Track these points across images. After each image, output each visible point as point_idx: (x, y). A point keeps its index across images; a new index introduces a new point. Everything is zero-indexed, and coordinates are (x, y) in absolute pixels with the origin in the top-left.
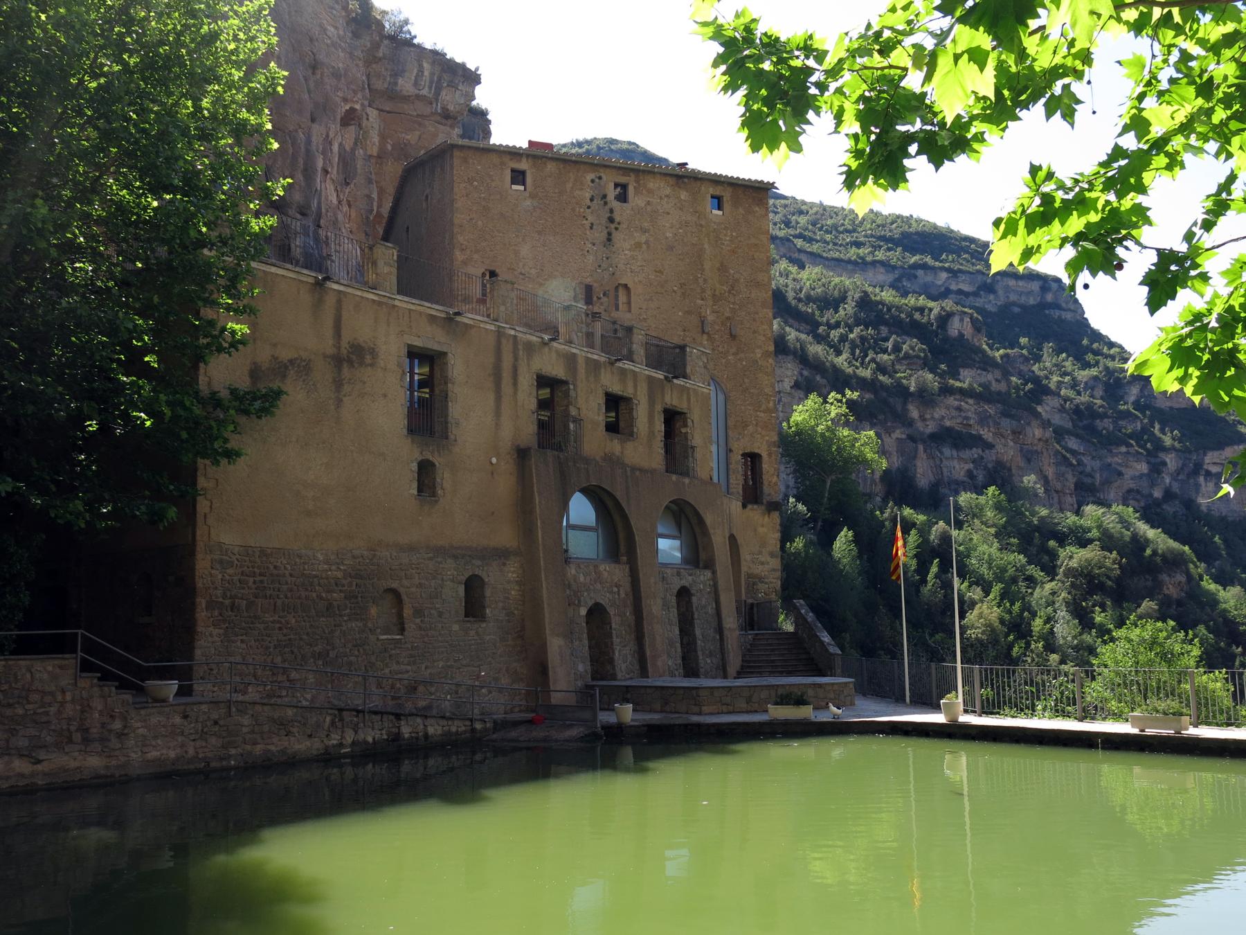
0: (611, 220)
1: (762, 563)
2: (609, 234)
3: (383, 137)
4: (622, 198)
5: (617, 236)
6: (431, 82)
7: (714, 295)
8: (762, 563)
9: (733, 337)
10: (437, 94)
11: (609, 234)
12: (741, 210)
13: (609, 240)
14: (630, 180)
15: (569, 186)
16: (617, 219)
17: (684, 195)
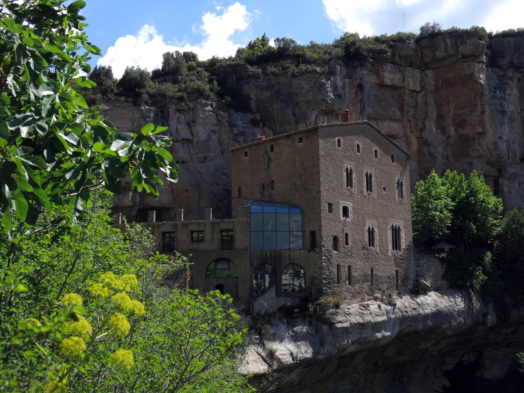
0: (269, 159)
1: (316, 272)
3: (436, 80)
4: (272, 150)
5: (271, 164)
6: (452, 46)
8: (316, 272)
9: (306, 189)
10: (457, 50)
12: (309, 140)
14: (274, 143)
16: (271, 158)
17: (290, 142)
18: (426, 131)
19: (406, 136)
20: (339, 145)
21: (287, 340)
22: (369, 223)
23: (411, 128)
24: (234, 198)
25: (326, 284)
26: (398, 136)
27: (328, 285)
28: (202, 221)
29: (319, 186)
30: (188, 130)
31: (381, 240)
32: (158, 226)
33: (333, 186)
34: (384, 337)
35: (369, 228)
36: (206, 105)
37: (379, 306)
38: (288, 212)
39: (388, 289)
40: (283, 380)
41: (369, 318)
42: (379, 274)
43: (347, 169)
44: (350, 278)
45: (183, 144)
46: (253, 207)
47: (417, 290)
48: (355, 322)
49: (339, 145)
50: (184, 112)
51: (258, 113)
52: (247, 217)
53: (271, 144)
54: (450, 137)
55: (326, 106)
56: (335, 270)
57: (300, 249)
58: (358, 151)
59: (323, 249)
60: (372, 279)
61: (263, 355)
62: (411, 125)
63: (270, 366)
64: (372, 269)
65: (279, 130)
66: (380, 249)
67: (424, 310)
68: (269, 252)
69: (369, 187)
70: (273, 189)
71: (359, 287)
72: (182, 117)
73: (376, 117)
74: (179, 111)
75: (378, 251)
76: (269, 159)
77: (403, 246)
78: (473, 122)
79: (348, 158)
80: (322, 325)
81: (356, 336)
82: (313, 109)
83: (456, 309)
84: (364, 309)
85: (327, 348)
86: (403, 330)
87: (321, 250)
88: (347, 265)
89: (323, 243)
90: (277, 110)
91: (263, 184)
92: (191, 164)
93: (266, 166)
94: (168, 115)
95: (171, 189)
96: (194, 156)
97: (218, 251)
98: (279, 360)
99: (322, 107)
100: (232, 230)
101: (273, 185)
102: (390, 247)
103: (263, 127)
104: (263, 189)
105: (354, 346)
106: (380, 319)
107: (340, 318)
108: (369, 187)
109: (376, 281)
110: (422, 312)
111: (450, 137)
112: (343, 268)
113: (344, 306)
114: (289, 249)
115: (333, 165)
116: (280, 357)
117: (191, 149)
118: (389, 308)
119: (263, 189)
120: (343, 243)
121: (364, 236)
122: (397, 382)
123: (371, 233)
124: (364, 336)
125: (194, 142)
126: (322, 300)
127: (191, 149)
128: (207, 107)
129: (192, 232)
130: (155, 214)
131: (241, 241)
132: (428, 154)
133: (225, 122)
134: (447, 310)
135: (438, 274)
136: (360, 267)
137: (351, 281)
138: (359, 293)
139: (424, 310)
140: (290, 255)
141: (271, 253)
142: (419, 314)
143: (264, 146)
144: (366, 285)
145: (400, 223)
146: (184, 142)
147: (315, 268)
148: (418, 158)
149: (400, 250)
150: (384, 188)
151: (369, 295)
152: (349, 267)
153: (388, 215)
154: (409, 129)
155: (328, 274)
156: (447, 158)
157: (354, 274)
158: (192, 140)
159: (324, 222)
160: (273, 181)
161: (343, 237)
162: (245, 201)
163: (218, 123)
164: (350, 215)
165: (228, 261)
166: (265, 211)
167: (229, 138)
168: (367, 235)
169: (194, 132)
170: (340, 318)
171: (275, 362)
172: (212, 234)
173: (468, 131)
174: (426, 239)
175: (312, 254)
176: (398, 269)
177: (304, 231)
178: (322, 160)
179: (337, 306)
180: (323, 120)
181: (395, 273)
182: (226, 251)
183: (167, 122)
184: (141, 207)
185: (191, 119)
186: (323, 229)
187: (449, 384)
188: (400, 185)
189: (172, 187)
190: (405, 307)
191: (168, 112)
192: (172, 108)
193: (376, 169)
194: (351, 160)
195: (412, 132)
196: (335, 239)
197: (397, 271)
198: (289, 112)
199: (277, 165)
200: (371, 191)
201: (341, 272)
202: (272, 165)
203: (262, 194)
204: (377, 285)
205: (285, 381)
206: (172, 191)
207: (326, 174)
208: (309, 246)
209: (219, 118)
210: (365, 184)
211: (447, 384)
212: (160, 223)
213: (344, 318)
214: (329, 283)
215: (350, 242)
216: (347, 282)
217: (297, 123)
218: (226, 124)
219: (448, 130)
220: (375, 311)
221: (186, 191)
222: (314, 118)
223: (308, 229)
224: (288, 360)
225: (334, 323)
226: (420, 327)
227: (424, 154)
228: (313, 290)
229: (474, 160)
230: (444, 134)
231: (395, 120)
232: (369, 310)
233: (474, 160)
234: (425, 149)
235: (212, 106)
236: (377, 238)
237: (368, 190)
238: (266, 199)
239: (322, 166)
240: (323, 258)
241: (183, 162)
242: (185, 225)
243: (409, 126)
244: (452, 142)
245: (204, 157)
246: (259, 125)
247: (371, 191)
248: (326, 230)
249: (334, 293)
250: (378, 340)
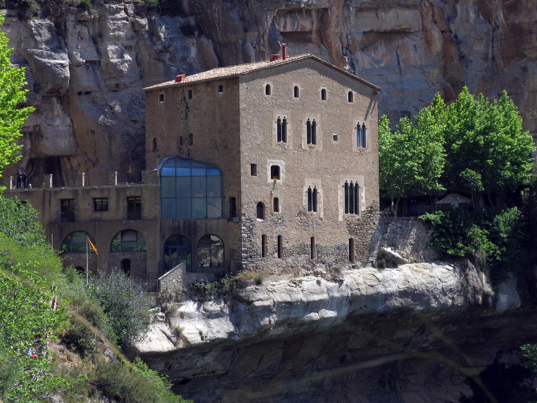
0: (187, 107)
1: (236, 244)
2: (187, 114)
4: (190, 97)
5: (188, 115)
7: (219, 130)
8: (236, 244)
9: (226, 148)
11: (187, 114)
12: (229, 89)
13: (187, 116)
15: (175, 97)
16: (189, 106)
17: (209, 89)
18: (458, 20)
19: (424, 29)
20: (268, 92)
21: (197, 319)
22: (309, 183)
23: (433, 16)
24: (149, 152)
25: (246, 258)
26: (411, 31)
27: (249, 259)
28: (105, 187)
29: (239, 145)
30: (94, 48)
31: (327, 202)
32: (56, 193)
33: (258, 143)
34: (323, 320)
35: (309, 190)
36: (118, 11)
37: (319, 283)
38: (204, 174)
39: (336, 262)
40: (196, 364)
41: (299, 296)
42: (323, 244)
43: (279, 120)
44: (280, 250)
45: (87, 67)
46: (165, 169)
47: (387, 262)
48: (280, 300)
49: (268, 92)
50: (86, 24)
51: (193, 15)
52: (157, 183)
53: (190, 89)
54: (498, 27)
55: (286, 5)
56: (259, 242)
57: (219, 218)
58: (296, 95)
59: (243, 218)
60: (312, 249)
61: (169, 333)
62: (433, 12)
63: (175, 344)
64: (312, 239)
65: (221, 40)
66: (324, 214)
67: (385, 287)
68: (182, 222)
69: (311, 138)
70: (191, 144)
71: (293, 260)
72: (85, 30)
73: (375, 6)
74: (80, 22)
75: (322, 216)
76: (187, 107)
78: (530, 5)
79: (280, 107)
80: (239, 303)
81: (282, 316)
82: (268, 10)
83: (439, 287)
84: (294, 285)
85: (244, 328)
86: (354, 311)
87: (240, 219)
88: (277, 235)
89: (243, 211)
90: (218, 12)
91: (181, 138)
92: (98, 95)
93: (184, 115)
94: (66, 30)
95: (71, 130)
96: (102, 83)
97: (124, 222)
98: (185, 340)
99: (281, 6)
100: (140, 197)
101: (192, 139)
102: (341, 210)
103: (199, 36)
104: (181, 144)
105: (282, 328)
106: (316, 298)
107: (260, 296)
108: (311, 138)
109: (318, 252)
110: (382, 290)
111: (498, 27)
112: (270, 238)
113: (268, 283)
114: (206, 218)
115: (258, 117)
116: (186, 335)
117: (98, 73)
118: (332, 284)
119: (181, 144)
120: (271, 209)
121: (302, 199)
122: (387, 387)
123: (312, 195)
124: (293, 316)
125: (102, 64)
126: (240, 276)
127: (98, 73)
128: (119, 13)
129: (95, 199)
130: (51, 179)
131: (150, 209)
132: (457, 57)
133: (144, 33)
134: (424, 288)
135: (420, 242)
136: (294, 236)
137: (281, 254)
138: (292, 267)
139: (385, 287)
140: (206, 225)
141: (184, 223)
142: (378, 293)
143: (181, 90)
144: (303, 259)
145: (360, 180)
146: (88, 64)
147: (235, 240)
148: (442, 63)
149: (357, 213)
150: (335, 138)
151: (308, 270)
152: (279, 237)
153: (340, 170)
154: (430, 18)
155: (249, 246)
156: (493, 59)
157: (285, 245)
158: (99, 62)
159: (245, 187)
160: (191, 135)
161: (270, 203)
162: (158, 160)
163: (134, 34)
164: (282, 175)
165: (136, 232)
166: (178, 175)
167: (150, 56)
168: (305, 198)
169: (102, 51)
170: (260, 296)
171: (181, 341)
172: (118, 201)
173: (522, 19)
174: (402, 199)
175: (230, 223)
176: (353, 237)
177: (223, 197)
178: (243, 114)
179: (258, 282)
180: (285, 23)
181: (348, 243)
182: (133, 222)
183: (65, 40)
184: (33, 156)
185: (97, 31)
186: (243, 195)
187: (472, 394)
188: (361, 130)
189: (73, 126)
190: (358, 284)
191: (65, 26)
192: (70, 20)
193: (322, 115)
194: (285, 108)
195: (435, 22)
196: (260, 206)
197: (351, 240)
198: (234, 15)
199: (195, 116)
200: (314, 143)
201: (267, 243)
202: (191, 115)
203: (180, 149)
204: (318, 258)
205: (198, 365)
206: (74, 132)
207: (249, 130)
208: (229, 214)
209: (137, 28)
210: (305, 135)
211: (469, 393)
212: (58, 189)
213: (266, 296)
214: (251, 257)
215: (280, 207)
216: (276, 255)
217: (246, 30)
218: (146, 36)
219: (494, 17)
220: (312, 287)
221: (93, 132)
222: (270, 22)
223: (228, 195)
224: (195, 339)
225: (253, 301)
226: (380, 308)
227: (451, 57)
228: (232, 265)
229: (530, 64)
230: (490, 22)
231: (408, 7)
232: (300, 287)
233: (530, 64)
234: (453, 50)
235: (126, 10)
236: (322, 200)
237: (309, 142)
238: (184, 156)
239: (243, 122)
240: (243, 228)
241: (88, 93)
242: (86, 191)
243: (431, 13)
244: (501, 34)
245: (117, 85)
246: (193, 34)
247: (314, 143)
248: (247, 196)
249: (257, 268)
250: (313, 322)
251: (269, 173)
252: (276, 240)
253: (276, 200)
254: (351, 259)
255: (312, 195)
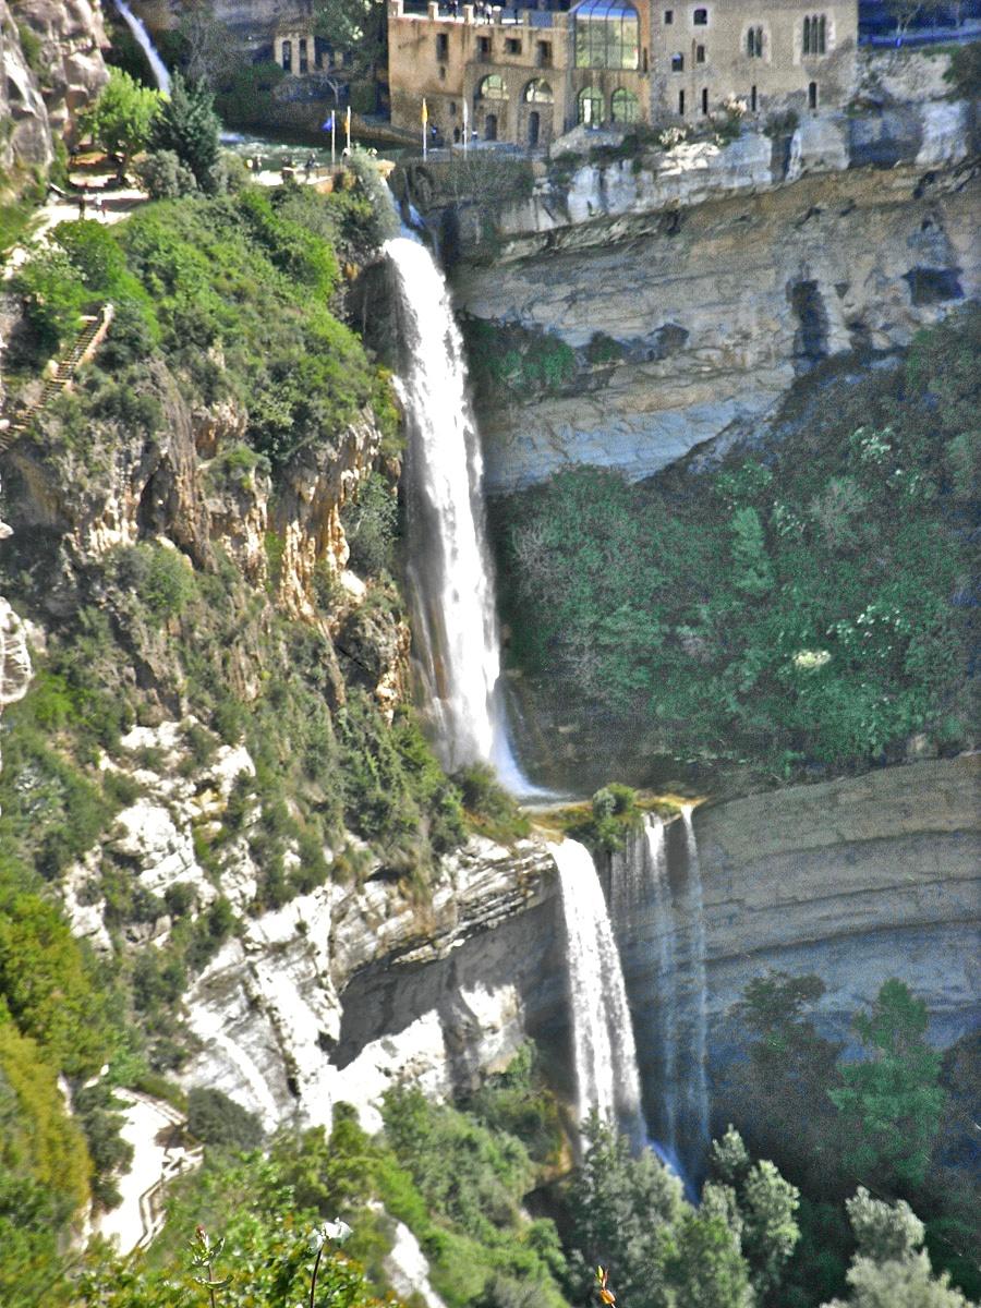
64: (754, 88)
77: (831, 46)
102: (798, 51)
181: (806, 88)
197: (813, 86)
216: (700, 111)
251: (691, 18)
252: (699, 96)
253: (701, 50)
254: (813, 105)
255: (755, 43)
